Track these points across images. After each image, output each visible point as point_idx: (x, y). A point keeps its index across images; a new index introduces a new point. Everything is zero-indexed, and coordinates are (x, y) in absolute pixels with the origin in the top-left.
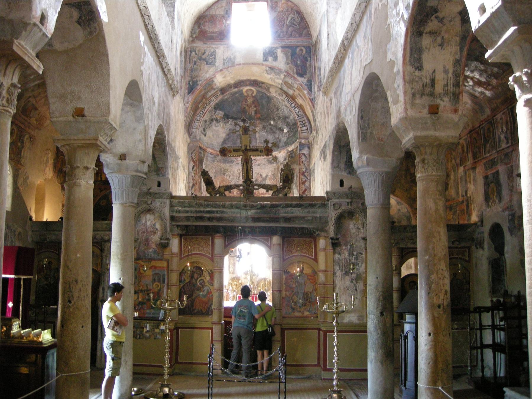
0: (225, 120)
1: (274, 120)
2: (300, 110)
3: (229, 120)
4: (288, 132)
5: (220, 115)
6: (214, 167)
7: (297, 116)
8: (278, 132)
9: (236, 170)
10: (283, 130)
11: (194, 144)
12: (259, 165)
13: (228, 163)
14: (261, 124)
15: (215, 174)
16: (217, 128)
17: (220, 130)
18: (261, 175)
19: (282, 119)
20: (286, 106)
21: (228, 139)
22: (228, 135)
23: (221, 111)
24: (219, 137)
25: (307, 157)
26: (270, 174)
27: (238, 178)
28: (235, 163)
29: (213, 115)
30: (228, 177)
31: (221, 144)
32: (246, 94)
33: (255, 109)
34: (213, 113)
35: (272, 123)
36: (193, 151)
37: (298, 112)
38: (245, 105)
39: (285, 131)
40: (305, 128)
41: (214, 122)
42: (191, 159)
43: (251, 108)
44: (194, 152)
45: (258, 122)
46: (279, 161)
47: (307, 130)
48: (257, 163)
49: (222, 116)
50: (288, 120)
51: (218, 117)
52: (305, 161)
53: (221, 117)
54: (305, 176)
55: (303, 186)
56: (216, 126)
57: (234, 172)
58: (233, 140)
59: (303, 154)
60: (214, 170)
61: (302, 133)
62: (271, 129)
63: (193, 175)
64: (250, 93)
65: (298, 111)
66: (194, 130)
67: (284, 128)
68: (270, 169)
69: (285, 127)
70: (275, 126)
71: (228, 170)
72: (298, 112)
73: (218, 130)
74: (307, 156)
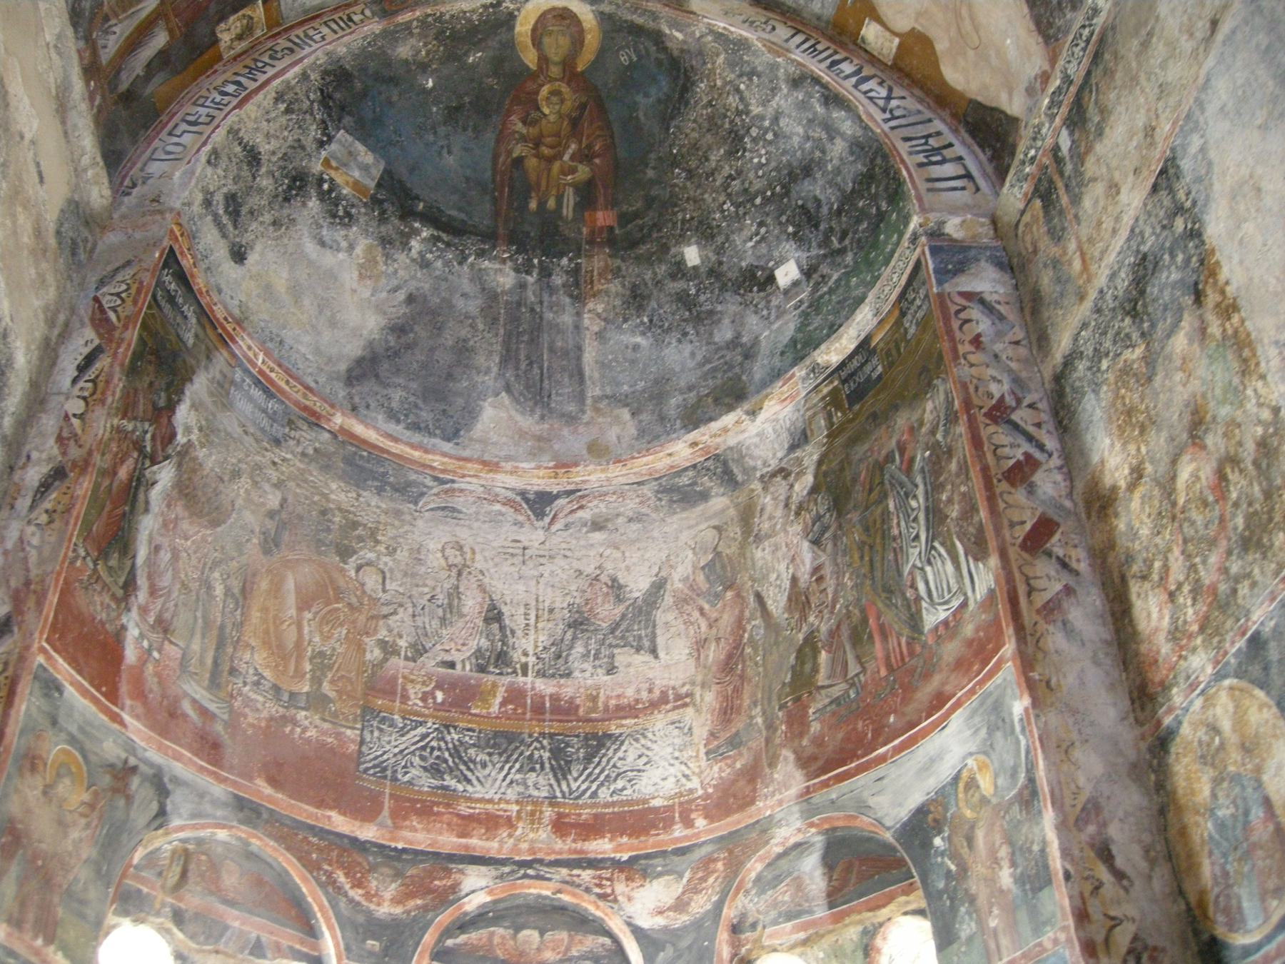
0: (383, 219)
1: (706, 232)
2: (898, 92)
3: (417, 232)
4: (808, 272)
5: (357, 174)
6: (274, 475)
7: (879, 116)
8: (731, 305)
9: (433, 545)
10: (771, 279)
11: (138, 235)
12: (597, 526)
13: (380, 491)
14: (617, 273)
15: (271, 525)
16: (329, 259)
17: (349, 277)
18: (616, 588)
19: (766, 201)
20: (799, 80)
21: (393, 354)
22: (399, 329)
23: (364, 142)
24: (333, 323)
25: (1002, 318)
26: (684, 569)
27: (442, 599)
28: (430, 501)
29: (309, 142)
30: (371, 581)
31: (343, 367)
32: (530, 58)
33: (583, 172)
34: (314, 132)
35: (692, 255)
36: (117, 270)
37: (889, 98)
38: (524, 139)
39: (787, 274)
40: (949, 169)
41: (314, 203)
42: (85, 309)
43: (556, 166)
44: (127, 274)
45: (598, 262)
46: (749, 471)
47: (968, 176)
48: (584, 515)
49: (372, 184)
50: (816, 189)
51: (339, 180)
52: (999, 335)
53: (356, 185)
54: (1016, 426)
55: (1020, 495)
56: (322, 243)
57: (417, 555)
58: (424, 366)
59: (968, 296)
60: (273, 500)
61: (929, 190)
62: (684, 300)
63: (76, 406)
64: (557, 46)
65: (884, 93)
66: (154, 168)
67: (779, 263)
68: (685, 536)
69: (789, 247)
70: (714, 272)
71: (373, 534)
72: (889, 98)
73: (331, 276)
74: (1002, 309)
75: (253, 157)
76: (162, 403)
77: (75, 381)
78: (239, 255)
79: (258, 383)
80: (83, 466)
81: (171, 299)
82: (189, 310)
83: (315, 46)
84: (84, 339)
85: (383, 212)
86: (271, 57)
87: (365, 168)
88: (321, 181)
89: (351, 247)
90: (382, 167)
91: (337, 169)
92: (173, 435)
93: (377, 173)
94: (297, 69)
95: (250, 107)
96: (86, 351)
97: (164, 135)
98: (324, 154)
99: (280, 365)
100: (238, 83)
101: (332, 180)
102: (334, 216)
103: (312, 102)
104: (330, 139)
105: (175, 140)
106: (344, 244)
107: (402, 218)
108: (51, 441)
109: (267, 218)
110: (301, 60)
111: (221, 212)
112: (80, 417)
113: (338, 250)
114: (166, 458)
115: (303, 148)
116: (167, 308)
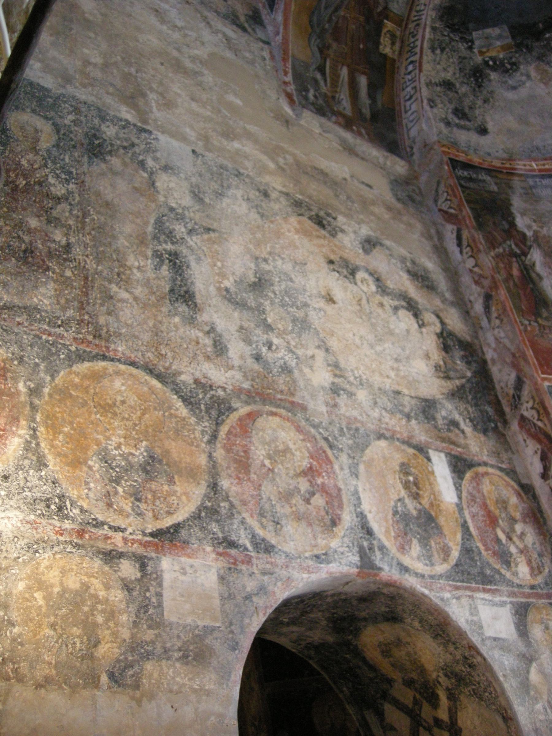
0: (530, 49)
5: (499, 43)
11: (432, 167)
16: (523, 92)
23: (487, 26)
34: (462, 46)
36: (437, 191)
41: (493, 76)
42: (439, 219)
44: (442, 188)
49: (509, 40)
51: (493, 54)
53: (504, 48)
56: (514, 88)
63: (470, 263)
66: (413, 132)
75: (448, 85)
76: (507, 226)
77: (461, 252)
78: (483, 131)
79: (543, 177)
80: (495, 286)
81: (470, 179)
82: (483, 176)
83: (425, 12)
84: (450, 231)
85: (527, 47)
86: (413, 37)
87: (500, 37)
88: (486, 63)
89: (528, 76)
90: (506, 28)
91: (488, 51)
92: (524, 235)
93: (506, 33)
94: (428, 30)
95: (426, 67)
96: (454, 235)
97: (404, 115)
98: (476, 50)
99: (546, 159)
100: (412, 62)
101: (491, 58)
102: (507, 71)
103: (448, 36)
104: (472, 41)
105: (410, 113)
106: (524, 78)
107: (538, 40)
108: (474, 286)
109: (479, 102)
110: (425, 25)
111: (457, 121)
112: (476, 265)
113: (524, 83)
114: (530, 248)
115: (465, 58)
116: (471, 185)
